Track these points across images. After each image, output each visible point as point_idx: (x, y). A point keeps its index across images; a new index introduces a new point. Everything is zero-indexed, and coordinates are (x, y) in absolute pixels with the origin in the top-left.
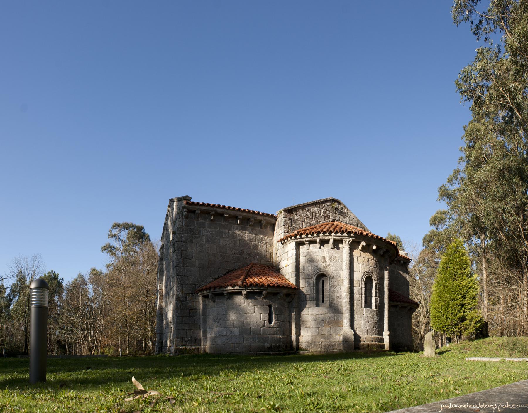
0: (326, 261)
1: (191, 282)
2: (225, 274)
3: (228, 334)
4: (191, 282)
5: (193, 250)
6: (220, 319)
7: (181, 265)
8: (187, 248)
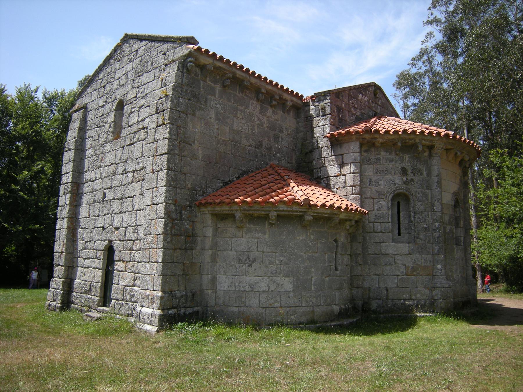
0: (406, 174)
1: (189, 186)
3: (271, 289)
4: (189, 186)
5: (196, 129)
6: (255, 260)
7: (176, 152)
8: (186, 123)
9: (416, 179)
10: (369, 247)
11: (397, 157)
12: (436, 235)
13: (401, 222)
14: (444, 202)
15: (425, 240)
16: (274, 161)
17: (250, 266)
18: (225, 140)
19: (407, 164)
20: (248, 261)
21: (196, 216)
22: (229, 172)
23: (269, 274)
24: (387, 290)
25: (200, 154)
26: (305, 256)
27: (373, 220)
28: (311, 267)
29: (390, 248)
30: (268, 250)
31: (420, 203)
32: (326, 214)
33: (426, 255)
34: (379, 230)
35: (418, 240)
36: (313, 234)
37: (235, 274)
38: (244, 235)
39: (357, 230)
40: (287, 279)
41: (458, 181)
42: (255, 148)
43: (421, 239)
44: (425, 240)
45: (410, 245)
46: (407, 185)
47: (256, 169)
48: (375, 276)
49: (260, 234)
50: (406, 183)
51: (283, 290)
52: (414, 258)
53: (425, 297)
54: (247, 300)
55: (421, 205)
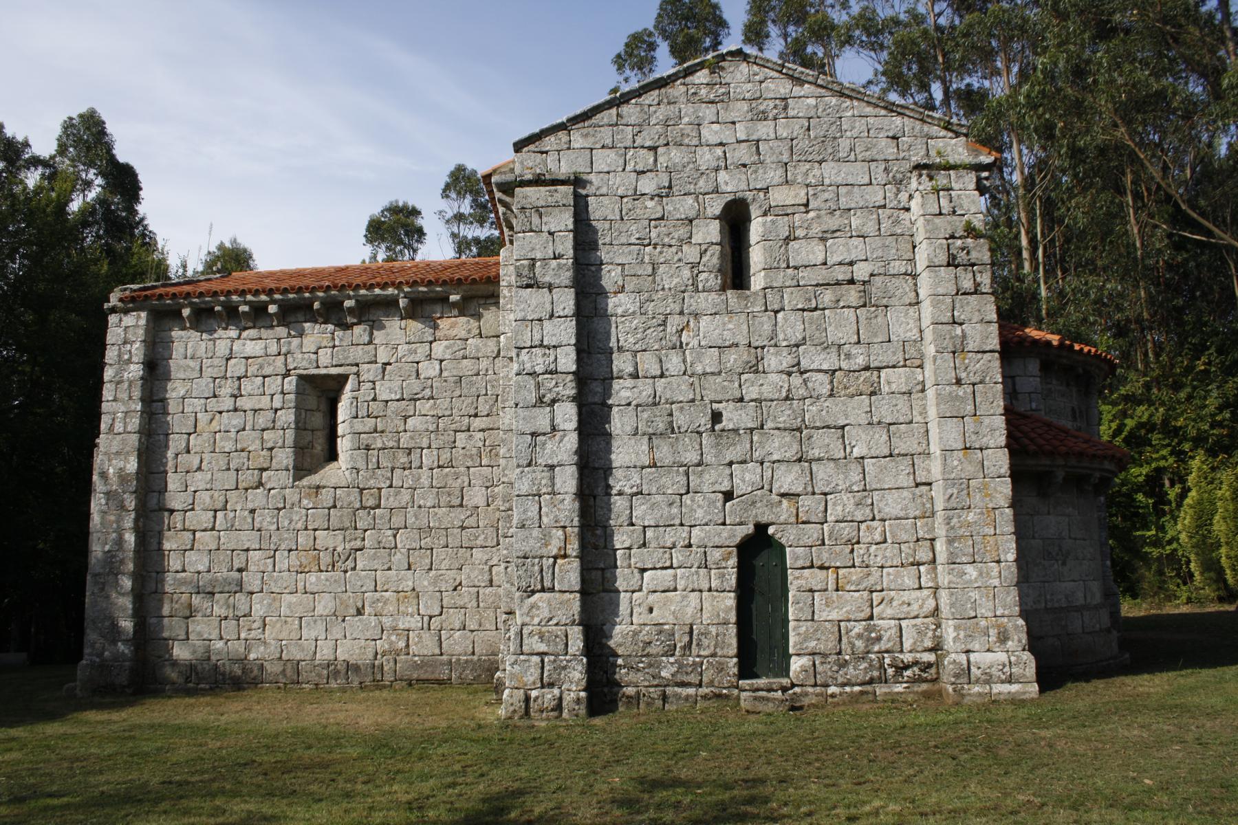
17: (1064, 564)
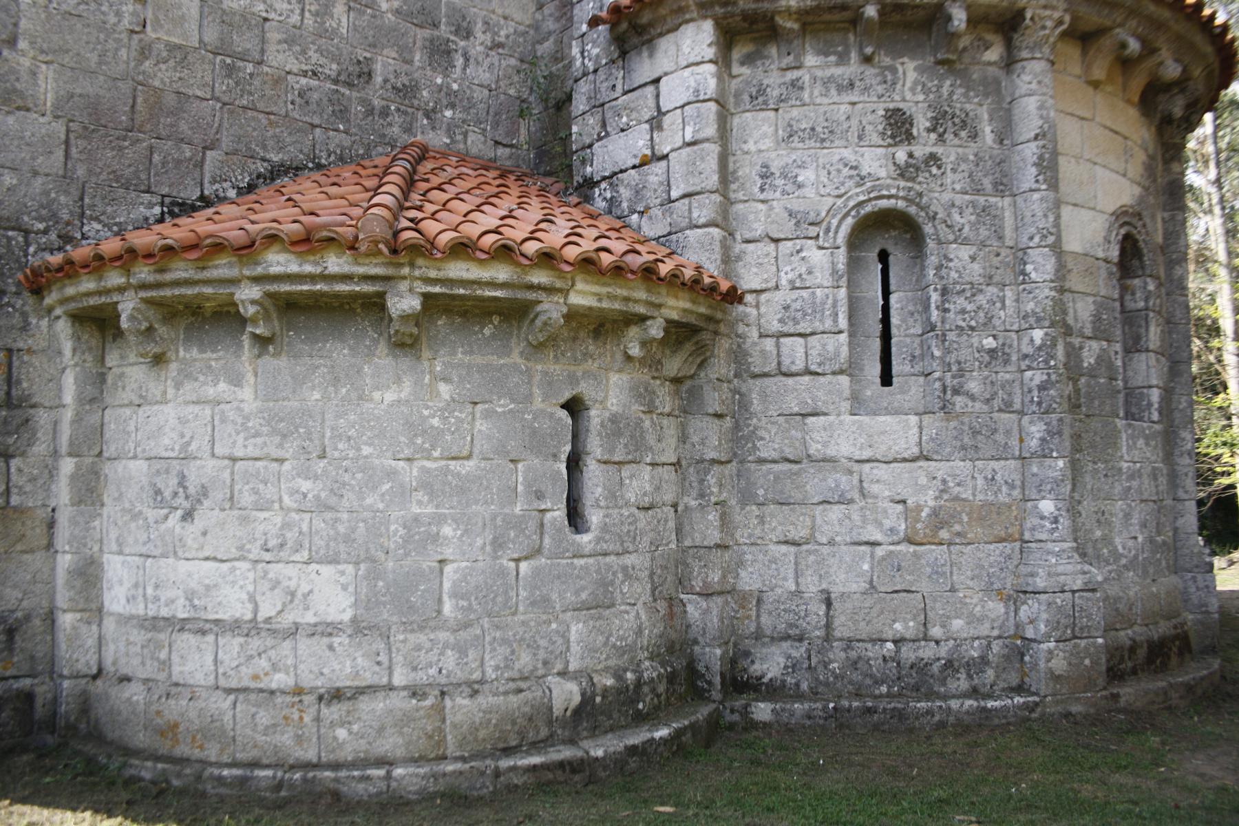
0: (910, 138)
2: (251, 188)
6: (204, 492)
9: (948, 154)
10: (761, 433)
11: (870, 71)
12: (1038, 377)
13: (894, 331)
14: (1073, 243)
15: (987, 401)
16: (431, 135)
17: (188, 516)
18: (179, 47)
19: (908, 96)
20: (180, 500)
21: (25, 327)
22: (201, 164)
23: (255, 552)
24: (829, 603)
25: (48, 86)
26: (411, 473)
27: (775, 326)
28: (440, 520)
29: (841, 435)
30: (251, 451)
31: (965, 253)
32: (492, 284)
33: (993, 458)
34: (799, 365)
35: (959, 400)
36: (446, 380)
37: (144, 550)
38: (171, 392)
39: (701, 365)
40: (327, 570)
41: (1136, 168)
42: (336, 81)
43: (973, 398)
44: (987, 401)
45: (926, 418)
46: (913, 180)
47: (341, 159)
48: (784, 548)
49: (222, 386)
50: (905, 172)
51: (310, 618)
52: (939, 475)
53: (984, 630)
54: (175, 658)
55: (973, 259)
